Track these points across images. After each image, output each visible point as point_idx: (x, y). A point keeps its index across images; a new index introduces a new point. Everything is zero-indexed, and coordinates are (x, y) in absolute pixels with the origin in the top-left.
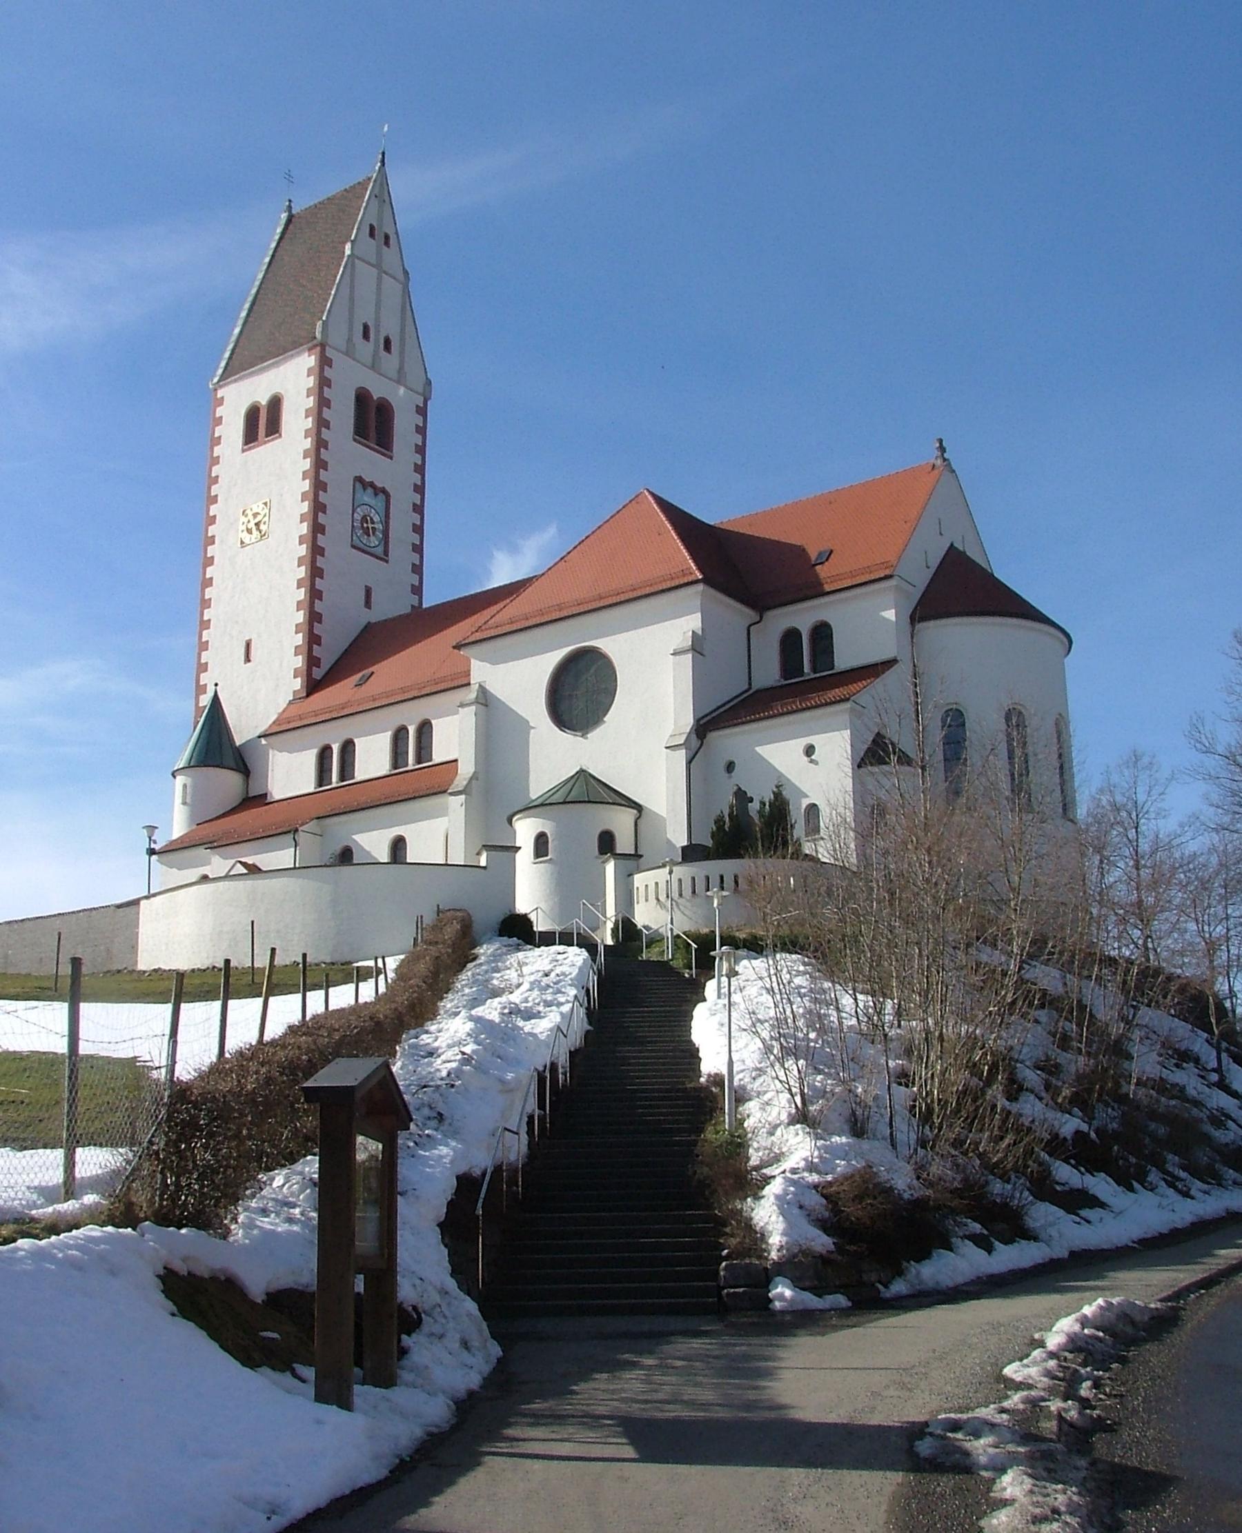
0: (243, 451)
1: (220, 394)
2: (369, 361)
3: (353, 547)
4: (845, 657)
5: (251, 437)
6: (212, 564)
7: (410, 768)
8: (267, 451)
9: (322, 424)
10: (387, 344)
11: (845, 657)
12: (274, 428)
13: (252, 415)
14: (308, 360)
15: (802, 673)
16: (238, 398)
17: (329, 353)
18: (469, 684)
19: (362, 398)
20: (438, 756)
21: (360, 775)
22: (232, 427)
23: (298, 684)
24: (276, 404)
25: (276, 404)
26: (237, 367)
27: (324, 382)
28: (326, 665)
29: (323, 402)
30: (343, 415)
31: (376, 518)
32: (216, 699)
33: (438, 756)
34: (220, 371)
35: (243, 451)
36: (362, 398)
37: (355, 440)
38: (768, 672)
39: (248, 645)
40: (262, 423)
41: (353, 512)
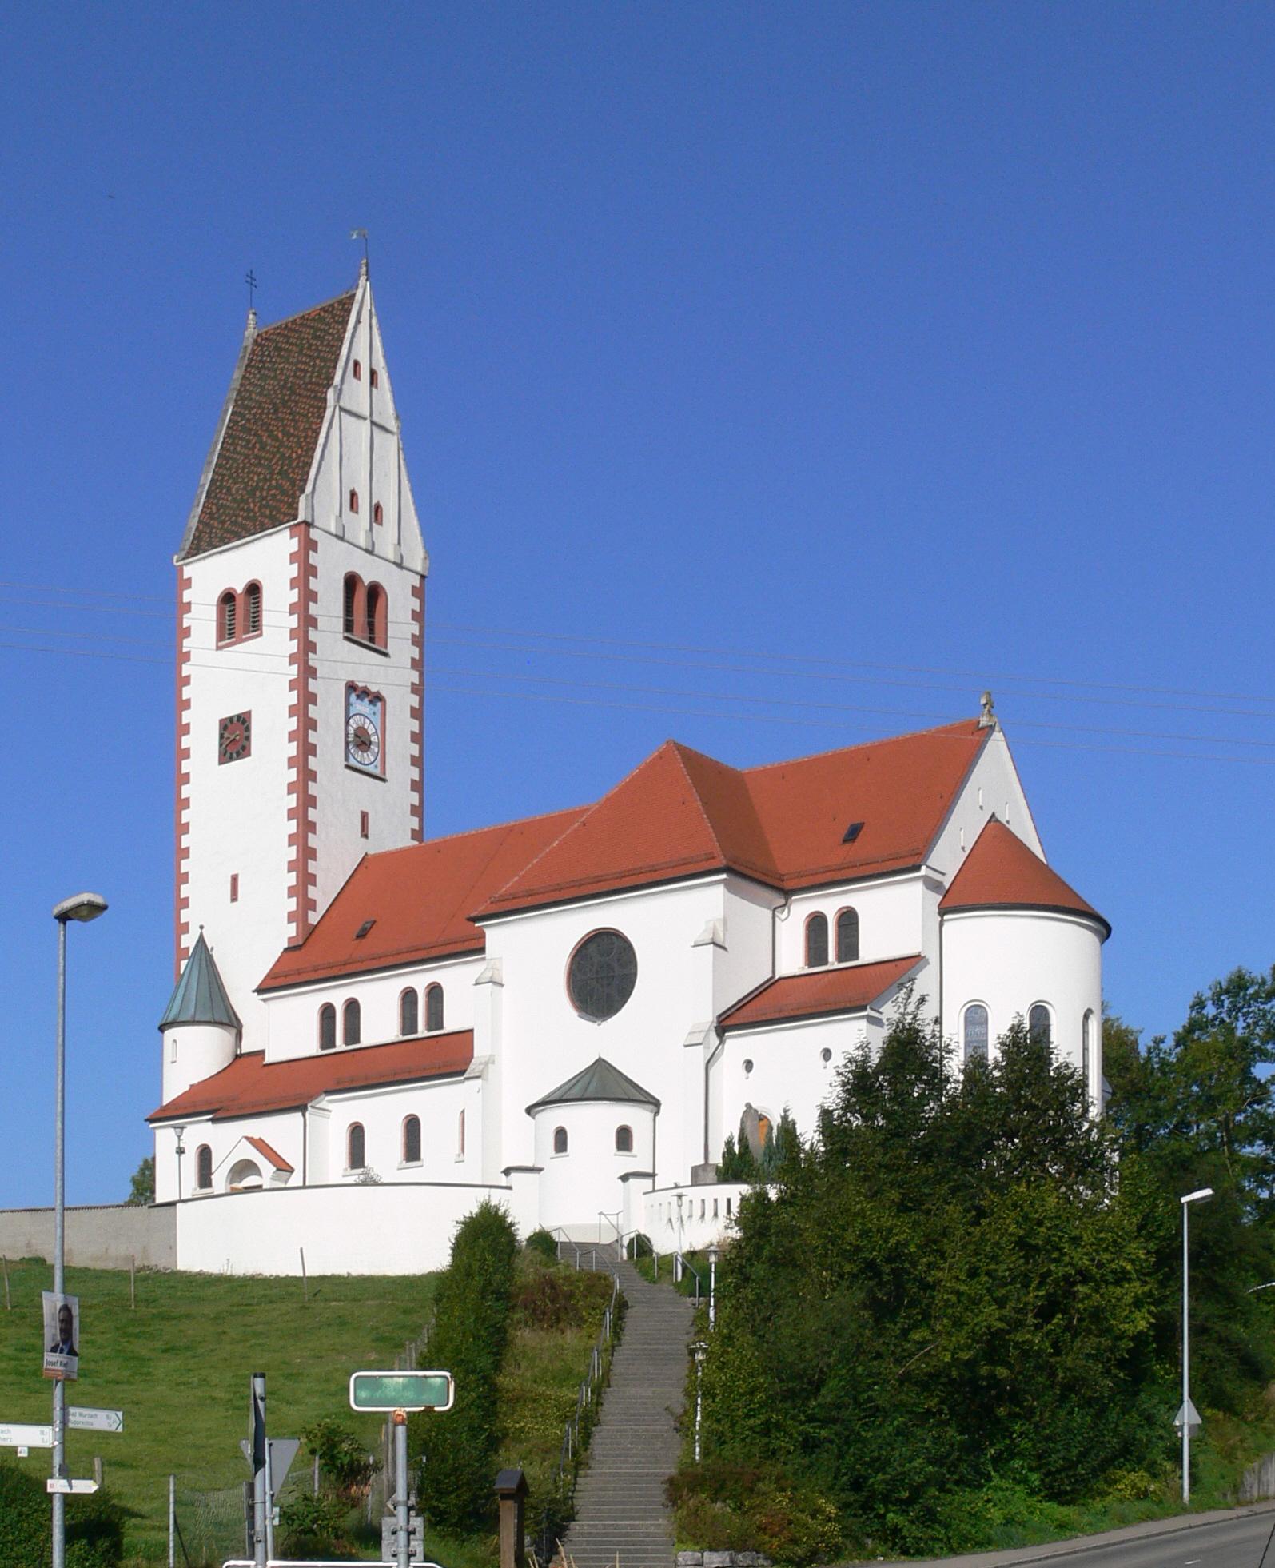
0: (218, 648)
2: (362, 541)
3: (348, 767)
4: (871, 949)
6: (187, 782)
7: (419, 1035)
8: (246, 651)
9: (308, 622)
10: (377, 512)
11: (871, 949)
12: (254, 624)
13: (228, 598)
15: (826, 963)
17: (314, 534)
18: (482, 950)
19: (351, 582)
20: (450, 1024)
21: (367, 1038)
22: (202, 620)
23: (291, 930)
24: (254, 589)
25: (254, 589)
27: (308, 571)
28: (322, 908)
31: (371, 730)
33: (450, 1024)
34: (188, 544)
38: (792, 960)
40: (240, 612)
41: (347, 723)
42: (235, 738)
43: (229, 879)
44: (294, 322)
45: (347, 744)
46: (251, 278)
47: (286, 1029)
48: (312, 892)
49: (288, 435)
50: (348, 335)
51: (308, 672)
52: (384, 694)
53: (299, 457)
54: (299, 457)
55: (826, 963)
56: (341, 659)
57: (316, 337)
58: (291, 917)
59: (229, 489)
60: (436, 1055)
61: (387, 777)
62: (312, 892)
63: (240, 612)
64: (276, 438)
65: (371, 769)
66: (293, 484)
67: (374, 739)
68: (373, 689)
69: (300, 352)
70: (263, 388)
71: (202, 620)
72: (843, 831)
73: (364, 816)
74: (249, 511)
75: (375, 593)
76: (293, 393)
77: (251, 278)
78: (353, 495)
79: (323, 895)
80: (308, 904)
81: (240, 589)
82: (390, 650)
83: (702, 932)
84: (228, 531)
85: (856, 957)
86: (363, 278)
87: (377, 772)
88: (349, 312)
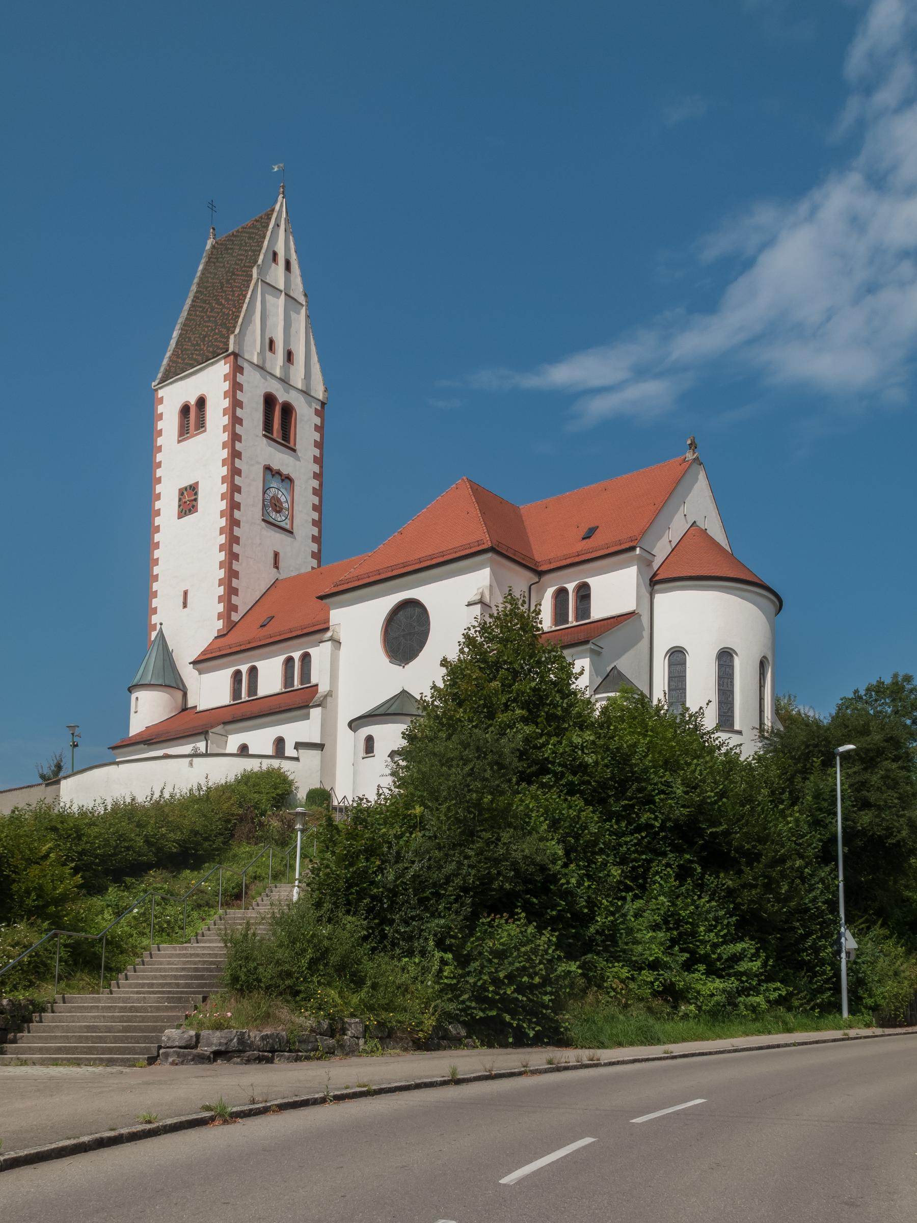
0: (179, 442)
1: (161, 393)
4: (599, 610)
5: (184, 432)
7: (296, 688)
8: (196, 442)
9: (236, 420)
11: (599, 610)
12: (201, 424)
13: (185, 410)
14: (222, 368)
15: (567, 622)
16: (173, 397)
17: (240, 362)
19: (269, 400)
20: (314, 680)
22: (169, 423)
23: (220, 624)
24: (201, 402)
25: (201, 402)
26: (174, 372)
27: (236, 386)
28: (242, 610)
29: (236, 404)
30: (253, 415)
32: (161, 631)
34: (160, 376)
35: (179, 442)
36: (269, 400)
37: (264, 436)
39: (186, 593)
40: (193, 417)
41: (264, 493)
42: (188, 501)
43: (182, 593)
44: (238, 231)
45: (264, 506)
46: (212, 206)
47: (211, 690)
48: (235, 600)
49: (227, 300)
50: (269, 233)
51: (235, 454)
52: (293, 476)
53: (233, 312)
54: (233, 312)
55: (567, 622)
56: (260, 451)
57: (250, 238)
58: (220, 616)
59: (190, 338)
60: (299, 699)
61: (295, 531)
62: (235, 600)
63: (193, 417)
64: (221, 304)
65: (282, 524)
66: (228, 330)
67: (285, 505)
68: (285, 471)
69: (240, 249)
70: (215, 274)
71: (169, 423)
72: (583, 531)
73: (276, 555)
74: (201, 350)
75: (288, 410)
76: (234, 274)
77: (212, 206)
78: (271, 342)
79: (243, 602)
80: (231, 608)
81: (193, 402)
82: (298, 447)
83: (473, 596)
84: (187, 364)
85: (589, 617)
86: (281, 196)
87: (288, 527)
88: (270, 219)
